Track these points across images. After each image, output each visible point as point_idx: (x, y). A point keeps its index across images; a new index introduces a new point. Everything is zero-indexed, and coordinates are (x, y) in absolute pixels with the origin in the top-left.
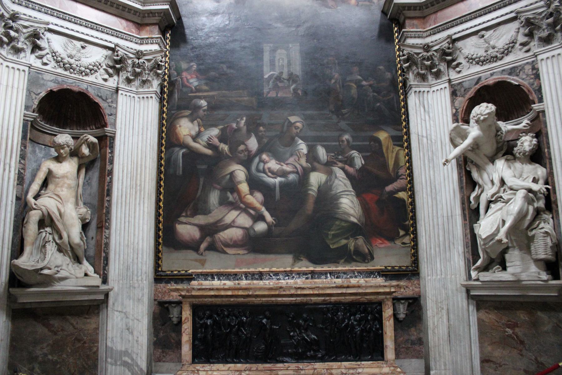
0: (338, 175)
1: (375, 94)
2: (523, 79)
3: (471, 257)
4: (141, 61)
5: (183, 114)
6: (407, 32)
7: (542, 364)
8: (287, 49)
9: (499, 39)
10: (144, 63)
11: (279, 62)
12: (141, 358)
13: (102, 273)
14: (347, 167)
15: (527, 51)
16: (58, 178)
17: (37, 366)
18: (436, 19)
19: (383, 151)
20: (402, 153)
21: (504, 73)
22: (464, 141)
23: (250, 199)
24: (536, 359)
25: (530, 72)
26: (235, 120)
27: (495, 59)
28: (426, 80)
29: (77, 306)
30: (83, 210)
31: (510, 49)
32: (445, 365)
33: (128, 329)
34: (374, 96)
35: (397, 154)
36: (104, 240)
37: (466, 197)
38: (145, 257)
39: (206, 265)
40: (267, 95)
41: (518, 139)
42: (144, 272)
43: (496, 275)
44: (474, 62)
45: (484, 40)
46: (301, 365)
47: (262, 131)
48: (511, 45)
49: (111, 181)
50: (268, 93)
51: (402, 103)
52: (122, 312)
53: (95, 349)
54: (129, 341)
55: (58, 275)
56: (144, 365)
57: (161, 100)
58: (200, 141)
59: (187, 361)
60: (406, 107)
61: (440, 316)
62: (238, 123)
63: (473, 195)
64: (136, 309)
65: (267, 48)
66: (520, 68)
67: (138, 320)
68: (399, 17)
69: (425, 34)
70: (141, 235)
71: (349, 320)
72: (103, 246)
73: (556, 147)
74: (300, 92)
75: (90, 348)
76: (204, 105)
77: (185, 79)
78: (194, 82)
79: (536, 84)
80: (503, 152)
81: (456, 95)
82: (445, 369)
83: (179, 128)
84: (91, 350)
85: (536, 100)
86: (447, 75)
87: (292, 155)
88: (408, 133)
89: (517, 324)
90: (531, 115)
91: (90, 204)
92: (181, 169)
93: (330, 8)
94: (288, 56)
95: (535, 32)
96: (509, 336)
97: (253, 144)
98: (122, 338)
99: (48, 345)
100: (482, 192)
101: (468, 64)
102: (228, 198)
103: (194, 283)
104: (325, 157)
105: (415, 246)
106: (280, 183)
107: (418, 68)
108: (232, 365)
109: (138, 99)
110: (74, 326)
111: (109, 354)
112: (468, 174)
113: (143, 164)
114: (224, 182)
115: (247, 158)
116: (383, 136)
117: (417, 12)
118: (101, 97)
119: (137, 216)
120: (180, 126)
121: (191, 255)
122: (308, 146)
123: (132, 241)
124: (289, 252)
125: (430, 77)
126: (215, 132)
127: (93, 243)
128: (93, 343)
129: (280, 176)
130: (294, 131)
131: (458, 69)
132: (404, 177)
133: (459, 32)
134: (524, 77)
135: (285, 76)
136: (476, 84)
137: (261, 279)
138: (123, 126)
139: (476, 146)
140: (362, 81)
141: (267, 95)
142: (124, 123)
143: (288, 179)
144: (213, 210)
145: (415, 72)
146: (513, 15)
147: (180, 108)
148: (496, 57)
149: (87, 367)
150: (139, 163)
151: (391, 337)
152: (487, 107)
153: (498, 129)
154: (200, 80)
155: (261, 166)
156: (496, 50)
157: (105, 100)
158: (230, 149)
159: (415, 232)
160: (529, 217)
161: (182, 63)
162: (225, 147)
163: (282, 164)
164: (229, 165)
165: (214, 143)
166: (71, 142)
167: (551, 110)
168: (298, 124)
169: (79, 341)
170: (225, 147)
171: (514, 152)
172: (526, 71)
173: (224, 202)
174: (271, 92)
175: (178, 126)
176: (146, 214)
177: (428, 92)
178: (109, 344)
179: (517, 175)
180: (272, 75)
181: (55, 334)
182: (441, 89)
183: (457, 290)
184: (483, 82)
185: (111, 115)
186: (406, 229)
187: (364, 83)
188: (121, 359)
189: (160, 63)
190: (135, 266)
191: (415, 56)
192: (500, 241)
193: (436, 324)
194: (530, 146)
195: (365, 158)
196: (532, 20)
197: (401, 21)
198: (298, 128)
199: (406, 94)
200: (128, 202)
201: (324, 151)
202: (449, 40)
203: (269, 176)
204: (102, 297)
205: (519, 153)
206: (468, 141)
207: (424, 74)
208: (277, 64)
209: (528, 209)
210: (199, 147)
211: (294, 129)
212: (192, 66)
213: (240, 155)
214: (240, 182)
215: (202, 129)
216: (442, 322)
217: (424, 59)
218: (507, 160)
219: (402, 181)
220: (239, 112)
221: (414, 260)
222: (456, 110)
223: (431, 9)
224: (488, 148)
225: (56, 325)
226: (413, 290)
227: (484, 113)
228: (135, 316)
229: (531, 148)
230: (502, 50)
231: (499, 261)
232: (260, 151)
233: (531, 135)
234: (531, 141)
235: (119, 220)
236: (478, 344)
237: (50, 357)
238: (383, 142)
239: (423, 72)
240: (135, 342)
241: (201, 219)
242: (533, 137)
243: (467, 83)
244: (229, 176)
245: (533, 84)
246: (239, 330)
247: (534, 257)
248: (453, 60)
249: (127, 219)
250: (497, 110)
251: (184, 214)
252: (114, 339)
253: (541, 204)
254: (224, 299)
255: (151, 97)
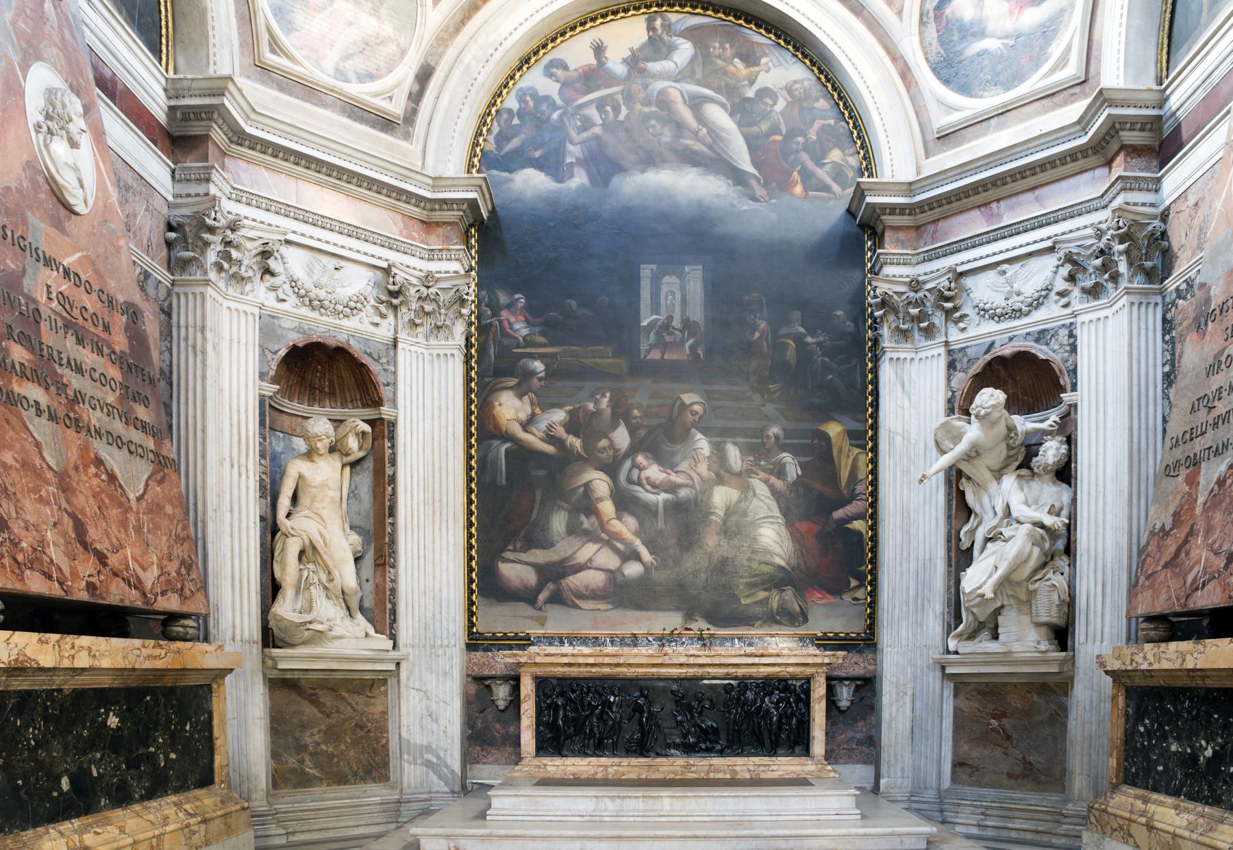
0: (757, 492)
1: (826, 359)
2: (1054, 351)
3: (953, 620)
4: (432, 290)
5: (504, 385)
6: (886, 254)
7: (1030, 763)
8: (681, 276)
9: (1027, 281)
10: (437, 294)
11: (666, 298)
12: (451, 755)
13: (388, 632)
14: (773, 479)
15: (1066, 306)
16: (315, 487)
17: (307, 758)
18: (935, 231)
19: (832, 455)
20: (864, 459)
21: (1029, 338)
22: (955, 445)
23: (616, 526)
24: (1024, 758)
25: (1065, 341)
26: (592, 397)
27: (1018, 314)
28: (909, 340)
29: (354, 680)
30: (355, 538)
31: (1041, 301)
32: (903, 770)
33: (431, 715)
34: (823, 362)
35: (855, 460)
36: (389, 585)
37: (953, 532)
38: (452, 611)
39: (548, 625)
40: (645, 356)
41: (1041, 444)
42: (451, 633)
43: (985, 645)
44: (987, 316)
45: (1007, 279)
46: (692, 761)
47: (636, 417)
48: (1044, 293)
49: (394, 494)
50: (648, 352)
51: (870, 376)
52: (421, 690)
53: (384, 741)
54: (433, 732)
55: (333, 633)
56: (456, 765)
57: (468, 358)
58: (534, 430)
59: (528, 753)
60: (875, 382)
61: (901, 703)
62: (596, 402)
63: (966, 528)
64: (441, 687)
65: (646, 271)
66: (1052, 332)
67: (445, 702)
68: (875, 224)
69: (914, 260)
70: (444, 577)
71: (763, 701)
72: (388, 593)
73: (1086, 462)
74: (700, 352)
75: (377, 740)
76: (539, 370)
77: (506, 323)
78: (521, 329)
79: (1070, 362)
80: (1017, 464)
81: (955, 369)
82: (902, 777)
83: (498, 408)
84: (378, 742)
85: (1069, 387)
86: (943, 334)
87: (685, 458)
88: (875, 427)
89: (1006, 713)
90: (1062, 409)
91: (360, 528)
92: (504, 476)
93: (755, 200)
94: (683, 288)
95: (1079, 276)
96: (994, 730)
97: (622, 438)
98: (422, 727)
99: (319, 732)
100: (979, 524)
101: (977, 318)
102: (582, 523)
103: (533, 649)
104: (739, 462)
105: (873, 605)
106: (666, 502)
107: (898, 319)
108: (594, 760)
109: (430, 358)
110: (353, 708)
111: (405, 749)
112: (962, 494)
113: (444, 466)
114: (574, 498)
115: (611, 461)
116: (834, 430)
117: (906, 217)
118: (370, 355)
119: (437, 549)
120: (500, 405)
121: (524, 609)
122: (710, 442)
123: (431, 586)
124: (678, 609)
125: (916, 334)
126: (559, 416)
127: (369, 587)
128: (381, 733)
129: (666, 491)
130: (690, 418)
131: (961, 325)
132: (864, 497)
133: (969, 261)
134: (1056, 347)
135: (676, 323)
136: (986, 353)
137: (635, 646)
138: (408, 403)
139: (974, 453)
140: (805, 336)
141: (645, 356)
142: (408, 398)
143: (677, 497)
144: (558, 542)
145: (893, 326)
146: (1049, 243)
147: (500, 373)
148: (1020, 310)
149: (374, 764)
150: (437, 464)
151: (821, 725)
152: (992, 395)
153: (1011, 429)
154: (534, 326)
155: (635, 476)
156: (1021, 298)
157: (377, 360)
158: (585, 445)
159: (874, 583)
160: (1032, 564)
161: (500, 294)
162: (575, 442)
163: (669, 471)
164: (584, 472)
165: (557, 435)
166: (329, 427)
167: (1086, 403)
168: (697, 408)
169: (362, 728)
170: (575, 442)
171: (1032, 465)
172: (1060, 338)
173: (573, 530)
174: (652, 351)
175: (497, 403)
176: (451, 545)
177: (912, 359)
178: (404, 734)
179: (1030, 501)
180: (656, 320)
181: (328, 716)
182: (933, 356)
183: (928, 667)
184: (999, 351)
185: (388, 384)
186: (861, 578)
187: (809, 339)
188: (422, 756)
189: (465, 297)
190: (438, 625)
191: (895, 297)
192: (982, 596)
193: (894, 715)
194: (1055, 456)
195: (803, 466)
196: (1075, 257)
197: (879, 230)
198: (697, 413)
199: (876, 360)
200: (422, 526)
201: (738, 452)
202: (950, 275)
203: (647, 491)
204: (392, 667)
205: (1038, 467)
206: (962, 447)
207: (906, 330)
208: (663, 302)
209: (1031, 552)
210: (533, 440)
211: (689, 414)
212: (518, 299)
213: (600, 455)
214: (600, 499)
215: (538, 411)
216: (904, 712)
217: (910, 303)
218: (1019, 476)
219: (859, 503)
220: (598, 384)
221: (870, 624)
222: (953, 392)
223: (929, 216)
224: (995, 457)
225: (328, 704)
226: (865, 668)
227: (987, 405)
228: (441, 696)
229: (1056, 459)
230: (1030, 300)
231: (992, 626)
232: (633, 451)
233: (1060, 439)
234: (1058, 449)
235: (409, 554)
236: (950, 743)
237: (324, 747)
238: (833, 440)
239: (905, 327)
240: (442, 733)
241: (539, 556)
242: (1061, 442)
243: (974, 349)
244: (582, 490)
245: (1067, 361)
246: (602, 712)
247: (1035, 620)
248: (956, 309)
249: (422, 553)
250: (1007, 400)
251: (511, 548)
252: (411, 727)
253: (1060, 544)
254: (582, 669)
255: (452, 355)
